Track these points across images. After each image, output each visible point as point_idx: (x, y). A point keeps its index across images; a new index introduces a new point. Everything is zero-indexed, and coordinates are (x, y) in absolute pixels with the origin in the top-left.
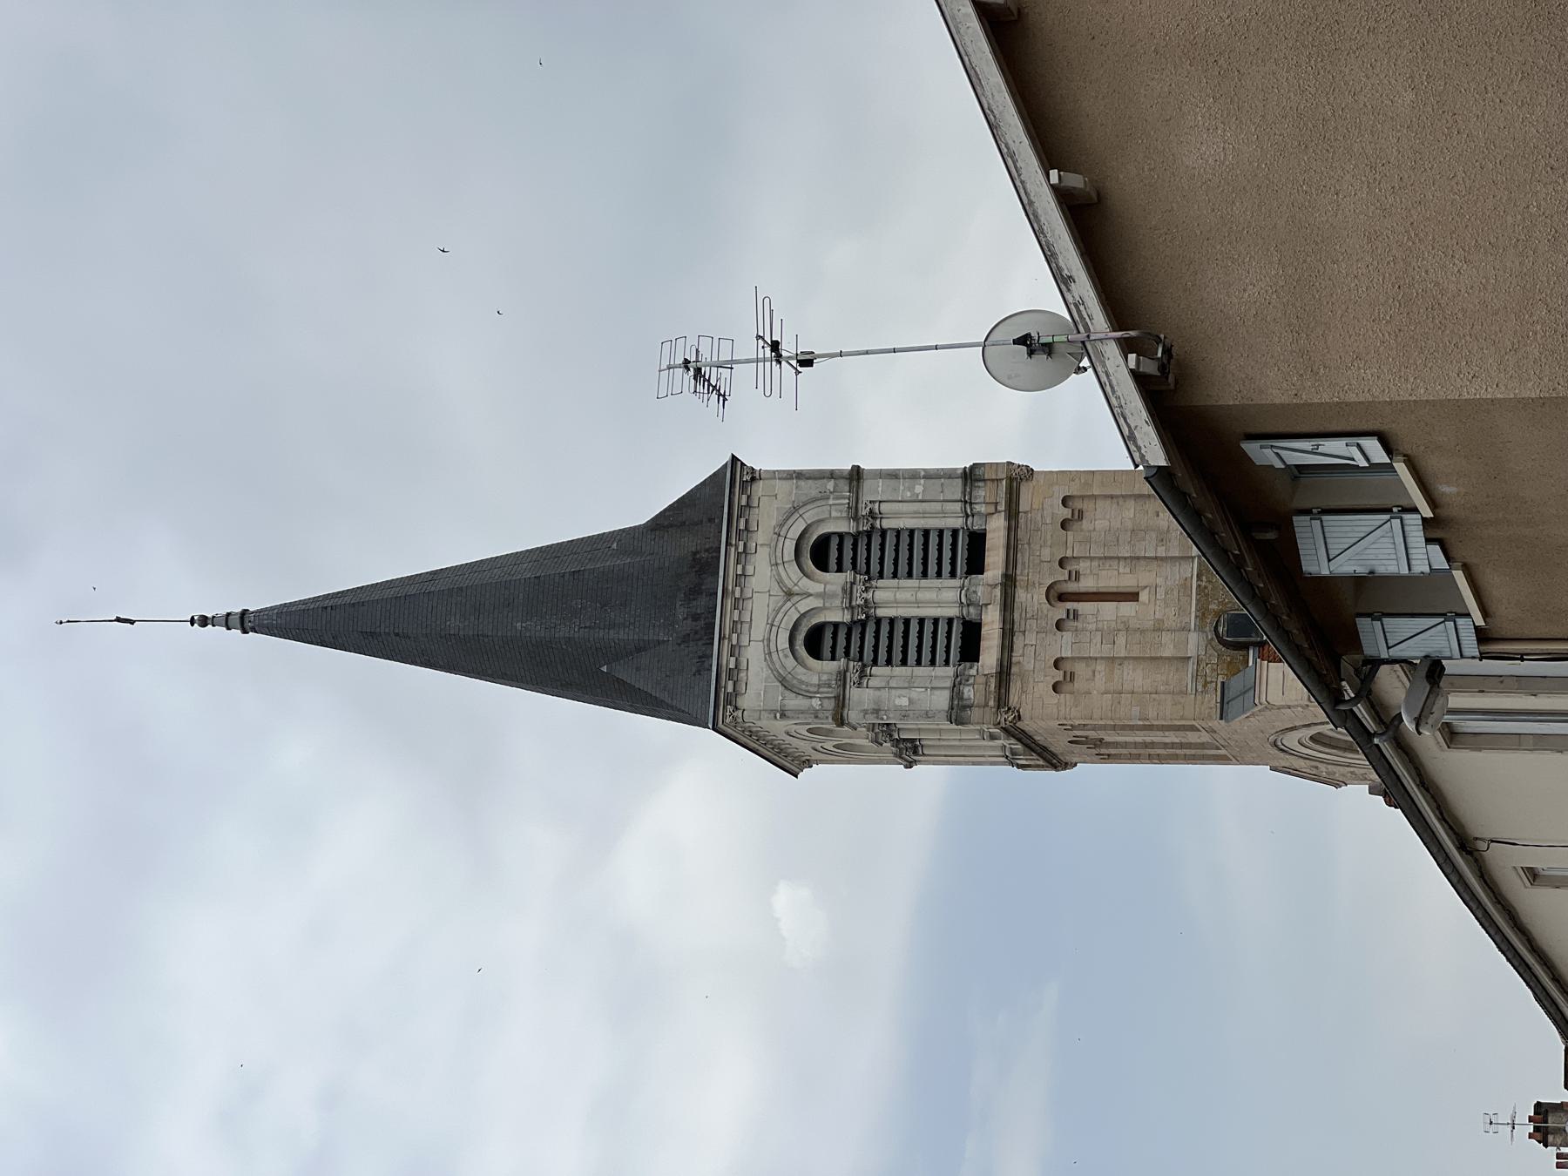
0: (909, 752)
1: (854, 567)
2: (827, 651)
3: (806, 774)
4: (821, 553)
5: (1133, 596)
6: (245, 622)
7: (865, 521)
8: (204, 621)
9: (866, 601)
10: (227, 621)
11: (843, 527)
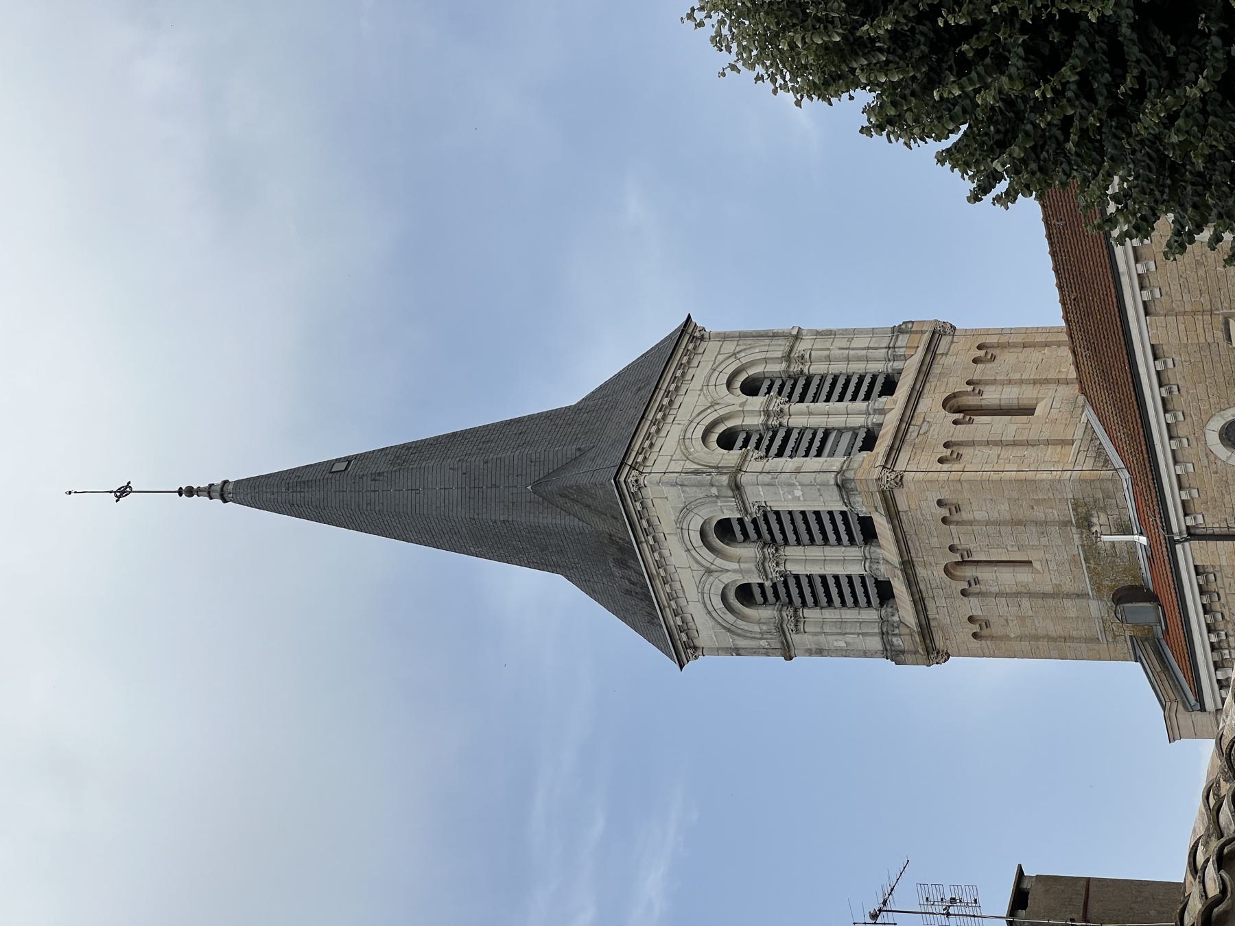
5: (1029, 411)
6: (223, 492)
7: (796, 365)
8: (190, 492)
9: (782, 410)
10: (209, 492)
11: (777, 368)
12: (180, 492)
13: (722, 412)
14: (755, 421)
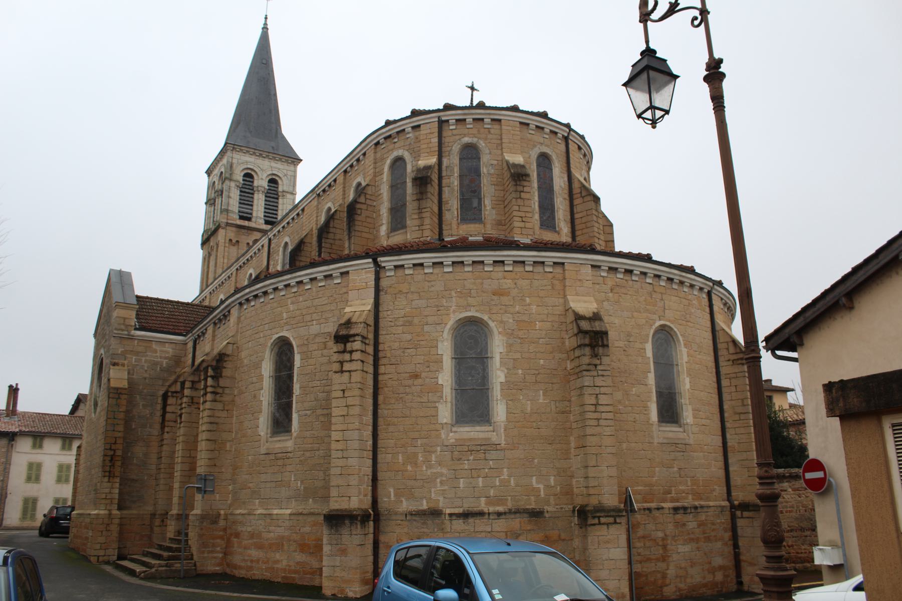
0: (210, 202)
1: (269, 189)
2: (245, 178)
3: (206, 175)
4: (273, 181)
6: (265, 29)
8: (266, 18)
9: (259, 191)
10: (266, 24)
11: (280, 189)
12: (266, 16)
13: (259, 173)
14: (256, 184)
